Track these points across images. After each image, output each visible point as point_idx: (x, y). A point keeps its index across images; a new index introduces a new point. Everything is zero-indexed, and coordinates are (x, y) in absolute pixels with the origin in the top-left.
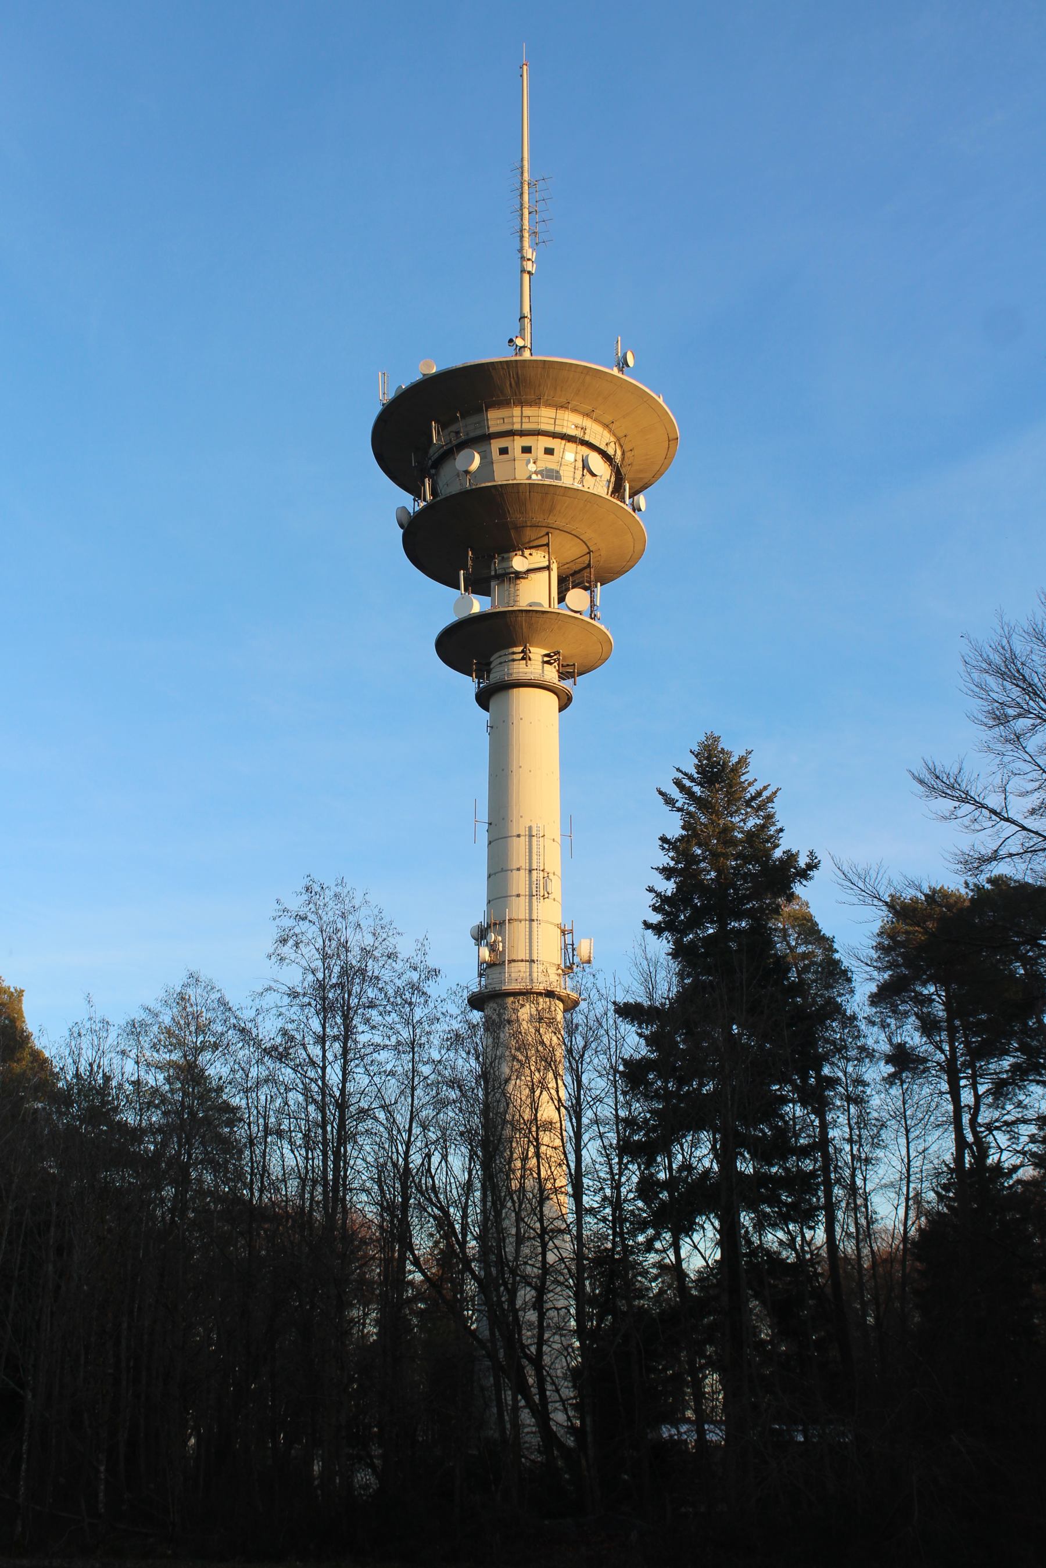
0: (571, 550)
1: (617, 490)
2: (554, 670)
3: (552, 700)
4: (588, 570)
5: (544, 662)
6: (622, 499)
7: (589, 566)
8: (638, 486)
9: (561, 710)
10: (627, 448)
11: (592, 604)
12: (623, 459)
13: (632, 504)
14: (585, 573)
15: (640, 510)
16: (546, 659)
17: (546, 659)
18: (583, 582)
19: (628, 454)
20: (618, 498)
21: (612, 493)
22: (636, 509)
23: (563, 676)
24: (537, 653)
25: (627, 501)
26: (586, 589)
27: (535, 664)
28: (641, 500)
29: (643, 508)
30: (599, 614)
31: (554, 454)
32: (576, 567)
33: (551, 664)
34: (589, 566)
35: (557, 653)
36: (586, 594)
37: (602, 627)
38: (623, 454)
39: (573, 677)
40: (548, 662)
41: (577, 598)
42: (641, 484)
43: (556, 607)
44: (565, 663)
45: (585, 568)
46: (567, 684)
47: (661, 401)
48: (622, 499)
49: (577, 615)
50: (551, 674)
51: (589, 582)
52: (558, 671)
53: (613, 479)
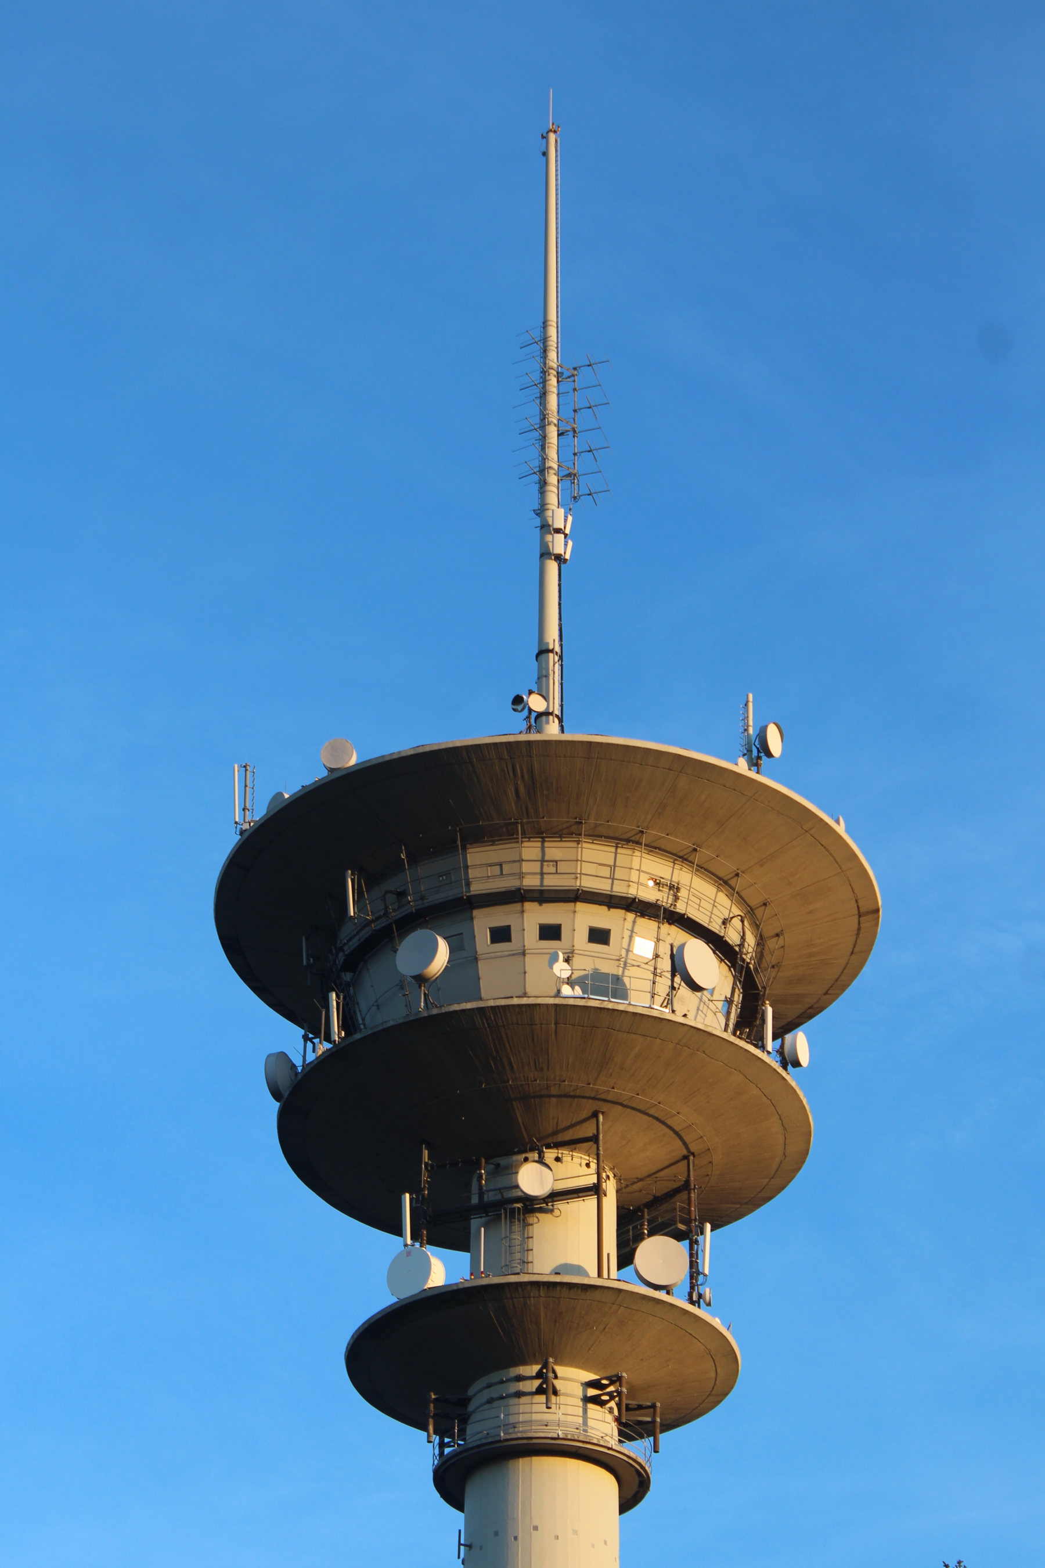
0: (650, 1151)
1: (748, 1021)
2: (609, 1418)
3: (604, 1487)
4: (684, 1195)
5: (587, 1400)
6: (759, 1041)
7: (686, 1186)
8: (792, 1012)
9: (626, 1505)
10: (768, 930)
11: (693, 1264)
12: (760, 955)
13: (781, 1052)
14: (678, 1203)
15: (797, 1064)
16: (592, 1392)
17: (592, 1392)
18: (673, 1222)
19: (772, 944)
20: (749, 1040)
21: (738, 1026)
22: (790, 1061)
23: (628, 1431)
24: (572, 1378)
25: (770, 1045)
26: (679, 1236)
27: (570, 1403)
28: (801, 1042)
29: (804, 1058)
30: (707, 1293)
31: (629, 946)
32: (658, 1189)
33: (602, 1404)
34: (686, 1186)
35: (615, 1379)
36: (681, 1249)
37: (716, 1322)
38: (761, 942)
39: (652, 1433)
40: (596, 1400)
41: (660, 1258)
42: (799, 1009)
43: (613, 1276)
44: (633, 1403)
45: (677, 1191)
46: (637, 1450)
47: (841, 829)
48: (759, 1041)
49: (661, 1295)
50: (602, 1426)
51: (687, 1222)
52: (618, 1420)
53: (738, 998)
